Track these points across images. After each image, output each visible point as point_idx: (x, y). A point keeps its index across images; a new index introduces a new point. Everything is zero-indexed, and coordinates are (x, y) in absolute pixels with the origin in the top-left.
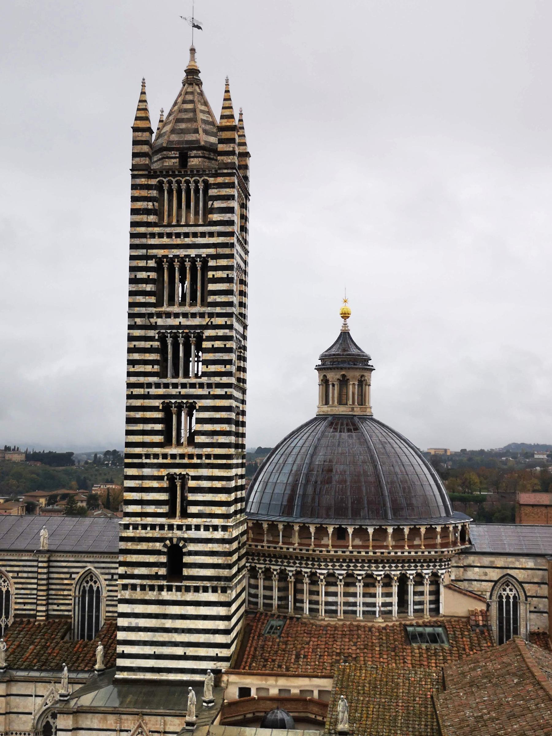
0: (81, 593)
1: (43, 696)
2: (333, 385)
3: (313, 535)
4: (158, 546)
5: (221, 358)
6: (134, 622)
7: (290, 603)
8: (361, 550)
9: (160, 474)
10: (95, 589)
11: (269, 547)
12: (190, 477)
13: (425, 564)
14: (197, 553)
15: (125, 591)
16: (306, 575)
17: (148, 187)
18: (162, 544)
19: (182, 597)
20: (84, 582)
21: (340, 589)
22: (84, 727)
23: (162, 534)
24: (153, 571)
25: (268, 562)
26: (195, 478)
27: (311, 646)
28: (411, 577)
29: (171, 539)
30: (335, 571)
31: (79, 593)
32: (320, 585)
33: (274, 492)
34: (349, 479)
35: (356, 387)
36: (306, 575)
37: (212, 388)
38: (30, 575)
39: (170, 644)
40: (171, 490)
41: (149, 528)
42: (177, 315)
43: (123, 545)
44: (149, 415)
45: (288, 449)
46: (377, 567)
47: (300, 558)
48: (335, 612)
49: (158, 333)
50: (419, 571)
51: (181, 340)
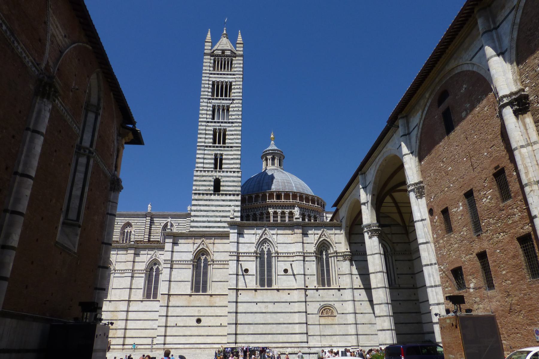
2: (270, 160)
4: (211, 179)
6: (199, 208)
14: (226, 181)
24: (207, 188)
26: (225, 155)
29: (215, 176)
38: (142, 224)
40: (216, 159)
41: (206, 172)
49: (213, 105)
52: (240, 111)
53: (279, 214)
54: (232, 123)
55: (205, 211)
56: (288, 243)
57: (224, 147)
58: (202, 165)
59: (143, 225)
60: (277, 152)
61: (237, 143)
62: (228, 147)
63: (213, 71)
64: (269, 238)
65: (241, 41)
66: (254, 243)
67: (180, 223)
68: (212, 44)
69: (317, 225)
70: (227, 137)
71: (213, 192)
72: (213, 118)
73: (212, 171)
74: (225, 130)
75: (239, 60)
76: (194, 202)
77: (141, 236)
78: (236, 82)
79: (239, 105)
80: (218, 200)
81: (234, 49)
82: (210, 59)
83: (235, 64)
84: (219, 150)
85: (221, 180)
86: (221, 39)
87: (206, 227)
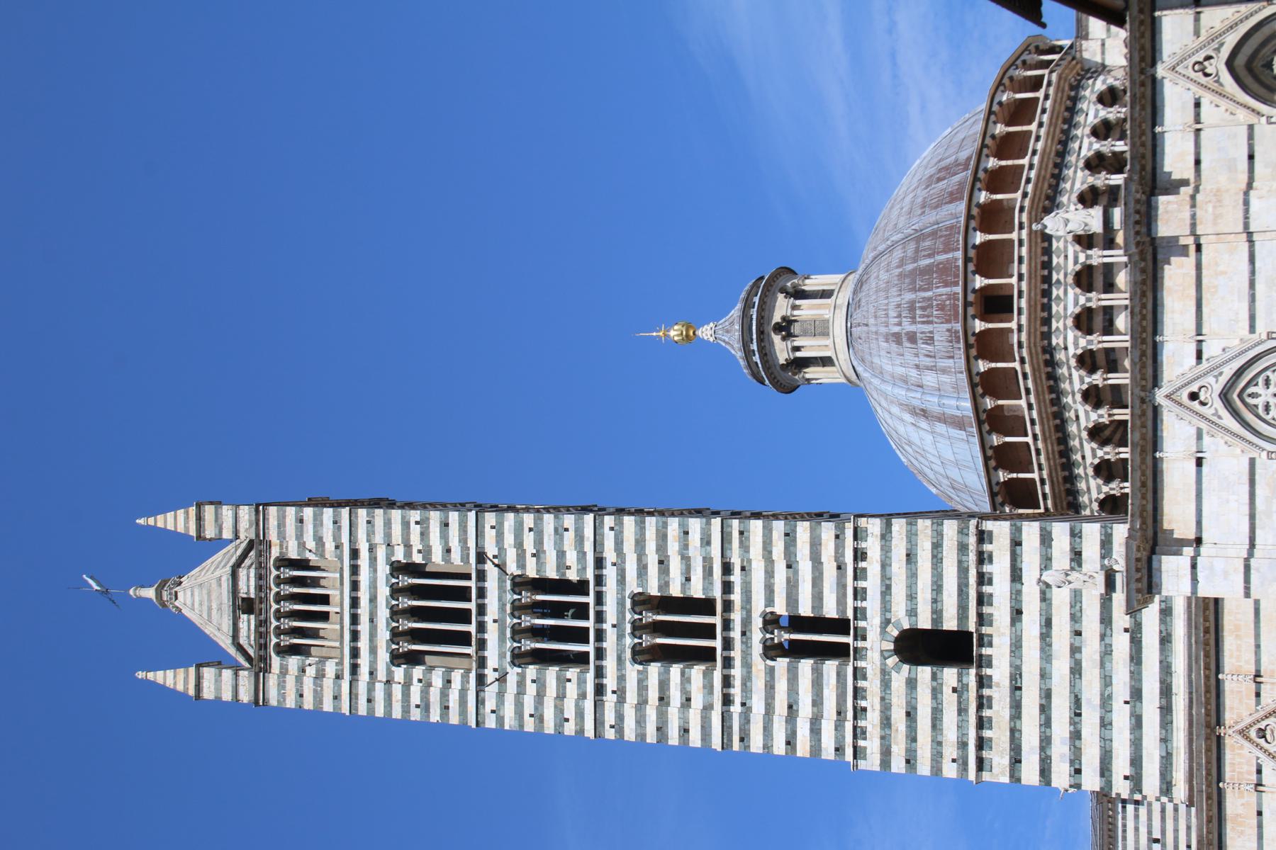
3: (993, 365)
5: (552, 537)
9: (762, 675)
14: (911, 597)
16: (1087, 380)
17: (284, 671)
18: (894, 674)
19: (1003, 634)
26: (770, 601)
29: (884, 655)
30: (1069, 313)
34: (909, 296)
35: (798, 302)
36: (1087, 380)
39: (1107, 664)
40: (797, 651)
41: (863, 704)
44: (653, 695)
49: (513, 663)
52: (539, 521)
53: (1089, 300)
54: (599, 563)
56: (1253, 272)
57: (728, 606)
58: (828, 728)
60: (754, 312)
61: (706, 541)
62: (727, 587)
63: (340, 663)
64: (1223, 380)
65: (187, 513)
66: (1252, 462)
67: (1150, 832)
68: (208, 665)
69: (1143, 108)
70: (675, 591)
71: (973, 671)
73: (859, 674)
74: (642, 602)
75: (281, 525)
76: (1030, 773)
78: (394, 542)
80: (1016, 646)
81: (230, 554)
83: (302, 545)
84: (744, 634)
85: (906, 626)
86: (186, 612)
87: (1166, 711)
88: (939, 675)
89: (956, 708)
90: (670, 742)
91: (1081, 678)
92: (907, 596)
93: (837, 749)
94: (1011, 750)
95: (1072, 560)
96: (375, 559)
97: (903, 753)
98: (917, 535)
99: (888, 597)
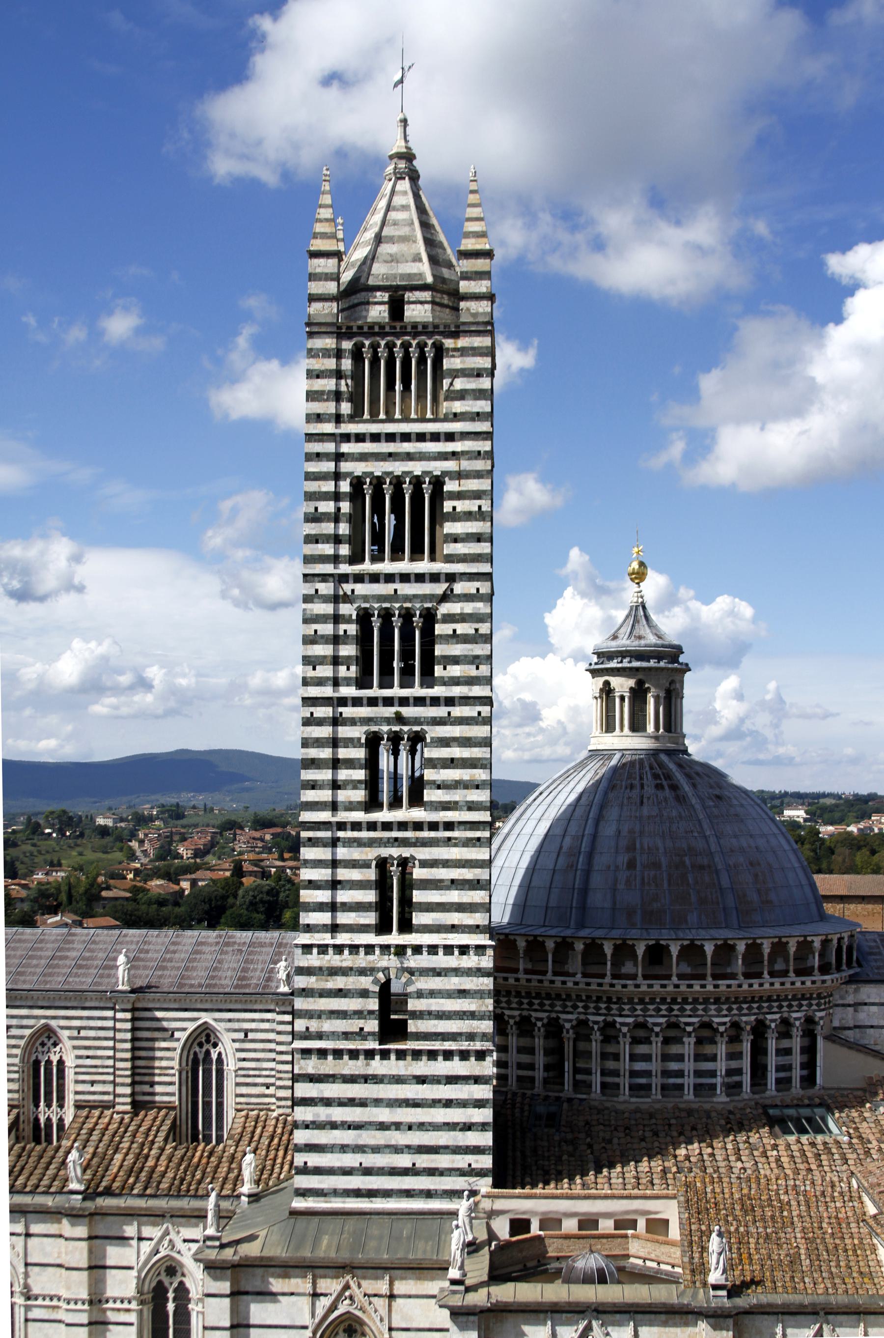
0: (190, 1063)
1: (151, 1239)
2: (622, 698)
3: (609, 957)
4: (365, 982)
5: (471, 653)
6: (322, 1113)
7: (566, 1074)
8: (692, 982)
9: (364, 857)
10: (214, 1056)
11: (528, 980)
12: (417, 862)
13: (795, 1003)
14: (432, 994)
15: (308, 1061)
16: (596, 1027)
18: (371, 978)
19: (407, 1069)
20: (195, 1045)
21: (655, 1048)
22: (249, 1288)
23: (370, 962)
25: (525, 1006)
26: (424, 864)
27: (616, 1147)
28: (773, 1025)
29: (386, 970)
30: (648, 1019)
31: (187, 1065)
32: (622, 1043)
33: (533, 884)
34: (664, 861)
36: (596, 1027)
37: (454, 705)
38: (102, 1034)
39: (388, 1150)
40: (382, 884)
41: (346, 952)
42: (390, 578)
43: (301, 982)
45: (550, 810)
46: (719, 1010)
47: (584, 998)
48: (648, 1087)
49: (359, 609)
50: (785, 1015)
51: (397, 621)
55: (350, 1126)
59: (106, 1039)
61: (472, 806)
67: (252, 1030)
72: (363, 682)
77: (104, 1082)
79: (480, 605)
80: (398, 1080)
82: (339, 354)
83: (456, 374)
84: (396, 839)
87: (357, 1193)
88: (372, 1016)
89: (348, 1030)
90: (303, 772)
91: (377, 1130)
92: (433, 990)
93: (308, 925)
94: (320, 1075)
95: (465, 1124)
96: (446, 459)
97: (309, 986)
98: (481, 998)
99: (431, 973)
